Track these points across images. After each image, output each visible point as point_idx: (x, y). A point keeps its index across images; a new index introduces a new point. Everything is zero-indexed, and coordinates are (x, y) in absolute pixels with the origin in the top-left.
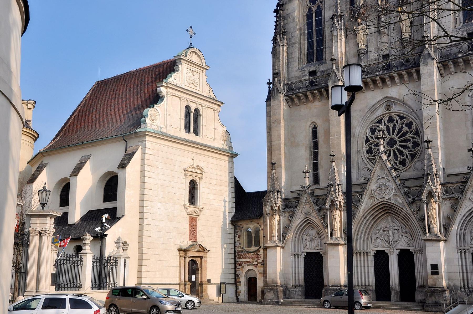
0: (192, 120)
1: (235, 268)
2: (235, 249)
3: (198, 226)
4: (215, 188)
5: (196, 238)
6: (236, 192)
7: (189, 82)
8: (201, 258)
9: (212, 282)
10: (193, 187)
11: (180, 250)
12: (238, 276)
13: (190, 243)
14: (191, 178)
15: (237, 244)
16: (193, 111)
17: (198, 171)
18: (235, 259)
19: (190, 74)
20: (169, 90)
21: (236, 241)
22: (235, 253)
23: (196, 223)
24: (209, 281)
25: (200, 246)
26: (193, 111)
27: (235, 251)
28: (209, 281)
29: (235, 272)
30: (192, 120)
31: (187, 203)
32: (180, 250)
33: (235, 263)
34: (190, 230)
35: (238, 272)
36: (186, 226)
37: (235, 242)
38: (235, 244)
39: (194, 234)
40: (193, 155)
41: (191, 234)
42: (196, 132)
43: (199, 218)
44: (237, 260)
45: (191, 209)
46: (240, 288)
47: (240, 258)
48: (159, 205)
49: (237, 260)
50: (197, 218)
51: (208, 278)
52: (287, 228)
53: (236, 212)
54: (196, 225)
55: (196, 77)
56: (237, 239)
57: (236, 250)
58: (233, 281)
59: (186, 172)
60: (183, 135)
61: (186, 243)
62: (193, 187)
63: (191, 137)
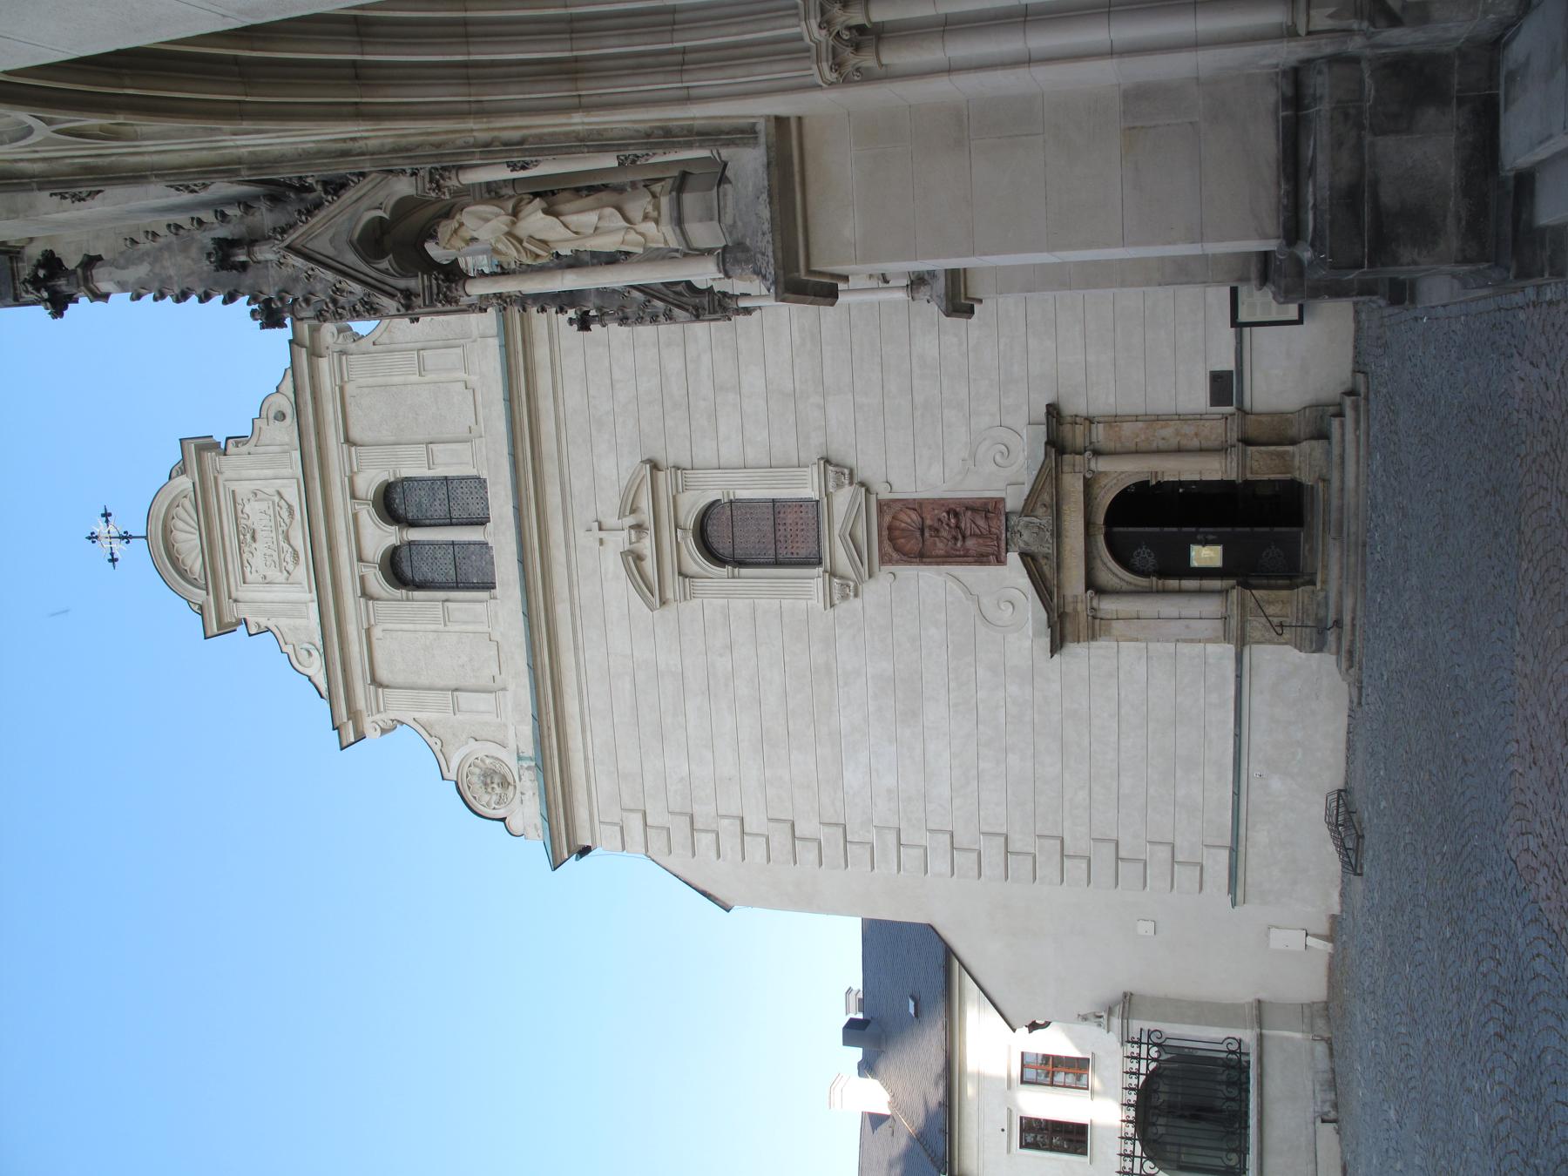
4: (706, 359)
7: (289, 558)
9: (1228, 364)
11: (1057, 646)
14: (694, 561)
17: (645, 503)
20: (361, 704)
24: (1223, 387)
31: (813, 582)
32: (1057, 646)
34: (948, 558)
36: (930, 581)
39: (966, 523)
40: (580, 533)
41: (970, 543)
43: (885, 495)
48: (853, 777)
50: (882, 506)
51: (1198, 398)
54: (917, 506)
55: (256, 514)
59: (669, 595)
63: (500, 537)
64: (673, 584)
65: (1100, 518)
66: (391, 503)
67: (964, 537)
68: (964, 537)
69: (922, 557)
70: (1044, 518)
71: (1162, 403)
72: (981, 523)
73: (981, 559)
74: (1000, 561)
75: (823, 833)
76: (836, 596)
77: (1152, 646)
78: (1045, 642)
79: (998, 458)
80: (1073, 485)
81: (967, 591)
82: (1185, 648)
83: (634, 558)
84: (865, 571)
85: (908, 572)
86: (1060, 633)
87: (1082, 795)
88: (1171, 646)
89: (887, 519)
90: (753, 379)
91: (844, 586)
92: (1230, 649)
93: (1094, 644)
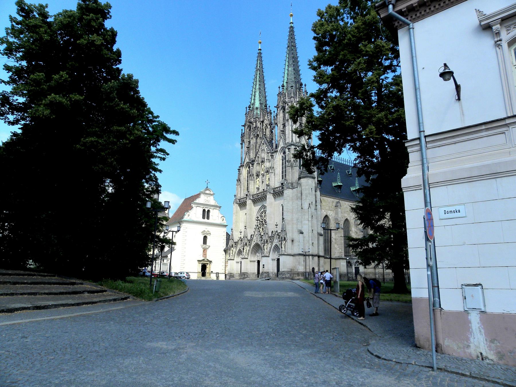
0: (206, 214)
10: (205, 238)
11: (198, 261)
13: (203, 258)
16: (206, 211)
19: (206, 198)
24: (212, 272)
26: (206, 211)
30: (206, 214)
42: (208, 218)
45: (204, 246)
52: (235, 252)
55: (209, 198)
60: (201, 220)
61: (201, 258)
62: (205, 238)
63: (206, 220)
66: (209, 211)
83: (204, 231)
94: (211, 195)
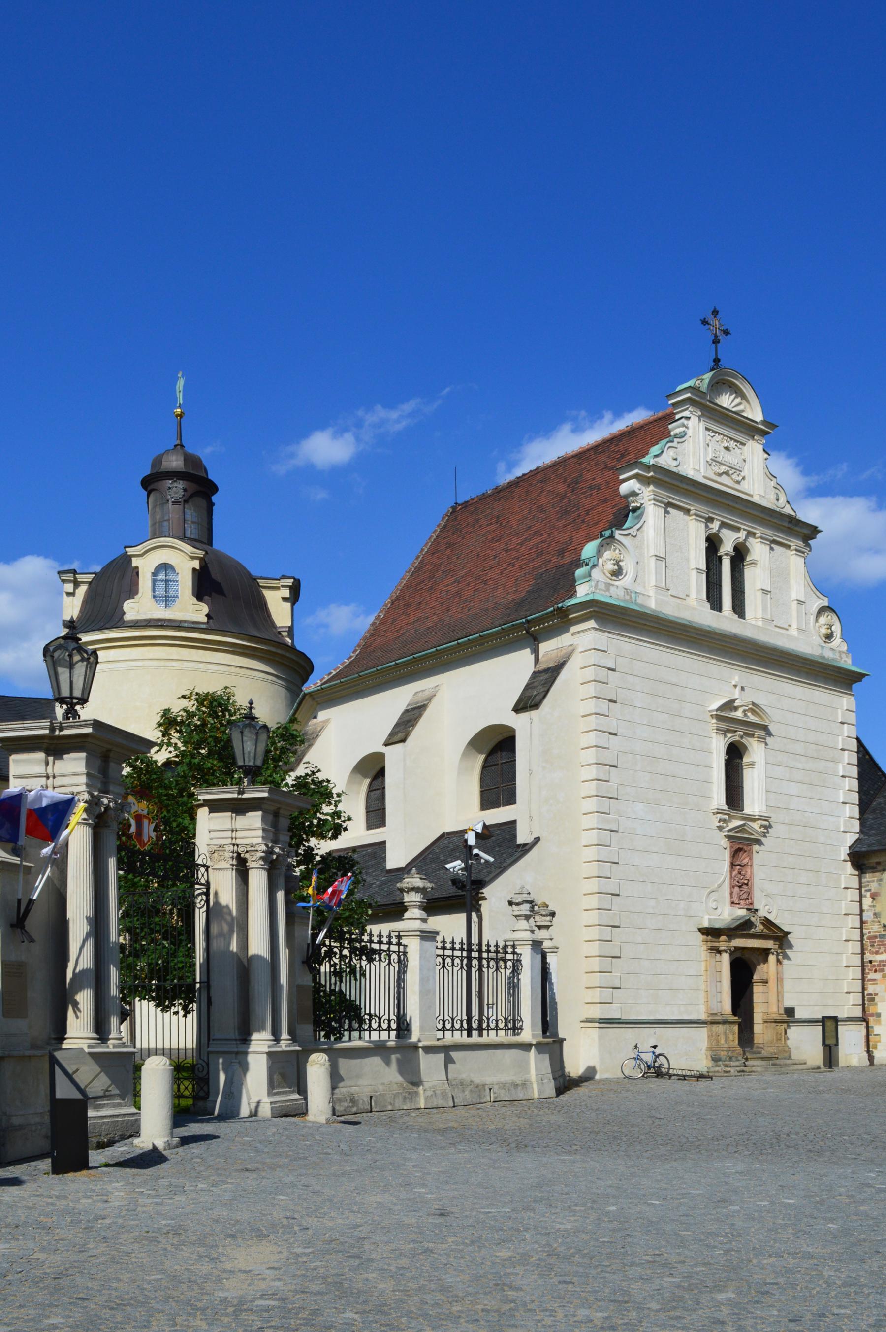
1: (863, 979)
2: (861, 928)
3: (755, 867)
5: (749, 897)
6: (861, 778)
8: (766, 952)
9: (798, 1015)
12: (872, 1000)
15: (868, 916)
18: (863, 954)
21: (865, 907)
22: (862, 940)
23: (751, 859)
25: (767, 922)
27: (862, 935)
28: (790, 1012)
29: (864, 989)
33: (863, 966)
35: (870, 989)
37: (862, 911)
38: (861, 915)
39: (745, 888)
41: (737, 889)
42: (739, 608)
44: (868, 956)
46: (877, 1029)
47: (877, 953)
49: (868, 956)
51: (788, 1004)
53: (861, 832)
56: (867, 901)
57: (865, 931)
58: (858, 1013)
64: (723, 725)
65: (747, 956)
67: (740, 887)
68: (740, 887)
69: (733, 865)
70: (759, 928)
71: (787, 985)
72: (745, 896)
73: (731, 894)
74: (733, 903)
75: (613, 784)
76: (719, 816)
77: (703, 978)
78: (706, 924)
79: (767, 907)
80: (769, 944)
81: (719, 886)
82: (702, 995)
84: (731, 834)
85: (727, 856)
86: (711, 933)
87: (639, 940)
88: (703, 987)
89: (745, 848)
90: (794, 789)
91: (724, 821)
92: (703, 1017)
93: (704, 948)
94: (749, 429)
